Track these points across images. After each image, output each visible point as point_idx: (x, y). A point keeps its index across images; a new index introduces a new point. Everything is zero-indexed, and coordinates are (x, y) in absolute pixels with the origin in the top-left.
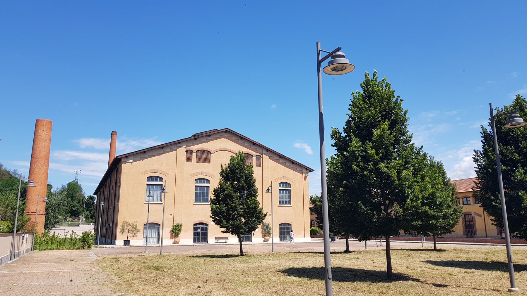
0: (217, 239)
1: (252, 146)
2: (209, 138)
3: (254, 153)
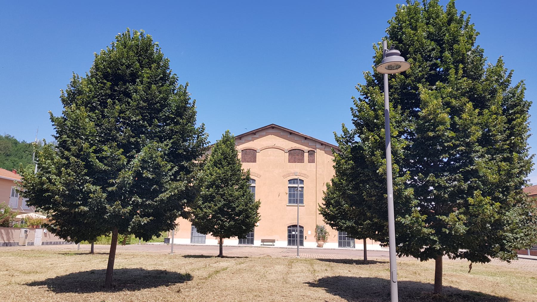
0: (263, 241)
1: (303, 141)
2: (255, 136)
3: (306, 149)
